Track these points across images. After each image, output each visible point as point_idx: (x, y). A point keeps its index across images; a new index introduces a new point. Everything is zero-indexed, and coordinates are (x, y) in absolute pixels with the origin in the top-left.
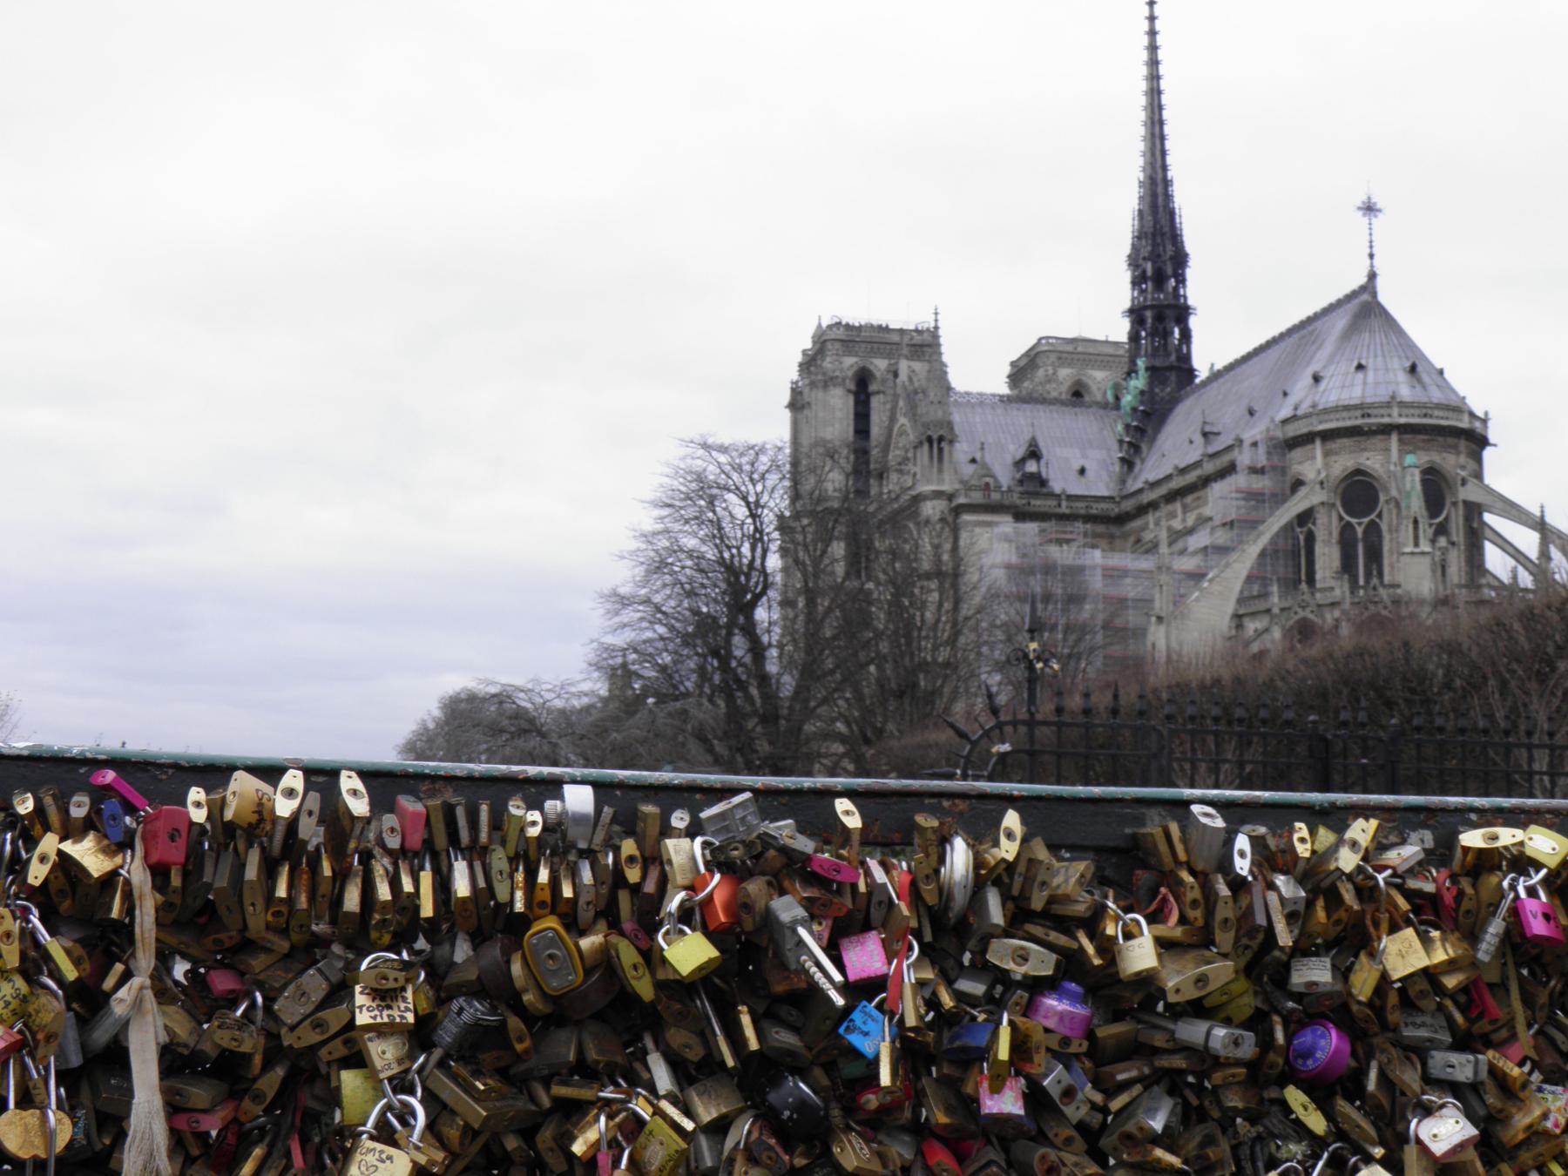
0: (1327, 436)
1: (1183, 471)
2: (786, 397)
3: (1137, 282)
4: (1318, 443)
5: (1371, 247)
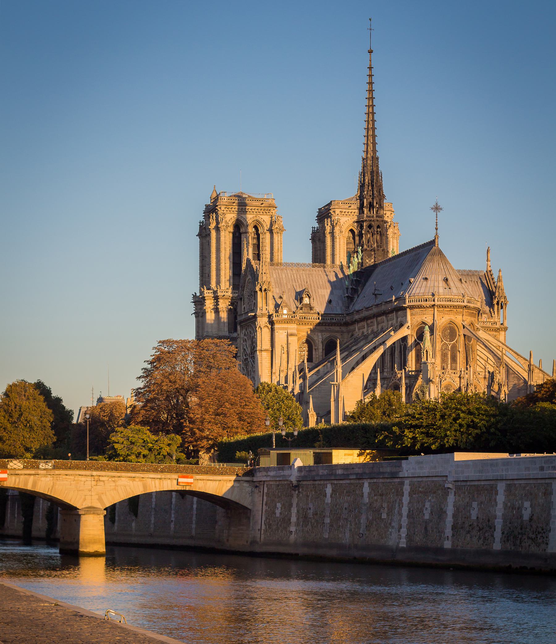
0: (412, 307)
1: (367, 309)
2: (197, 231)
5: (437, 225)
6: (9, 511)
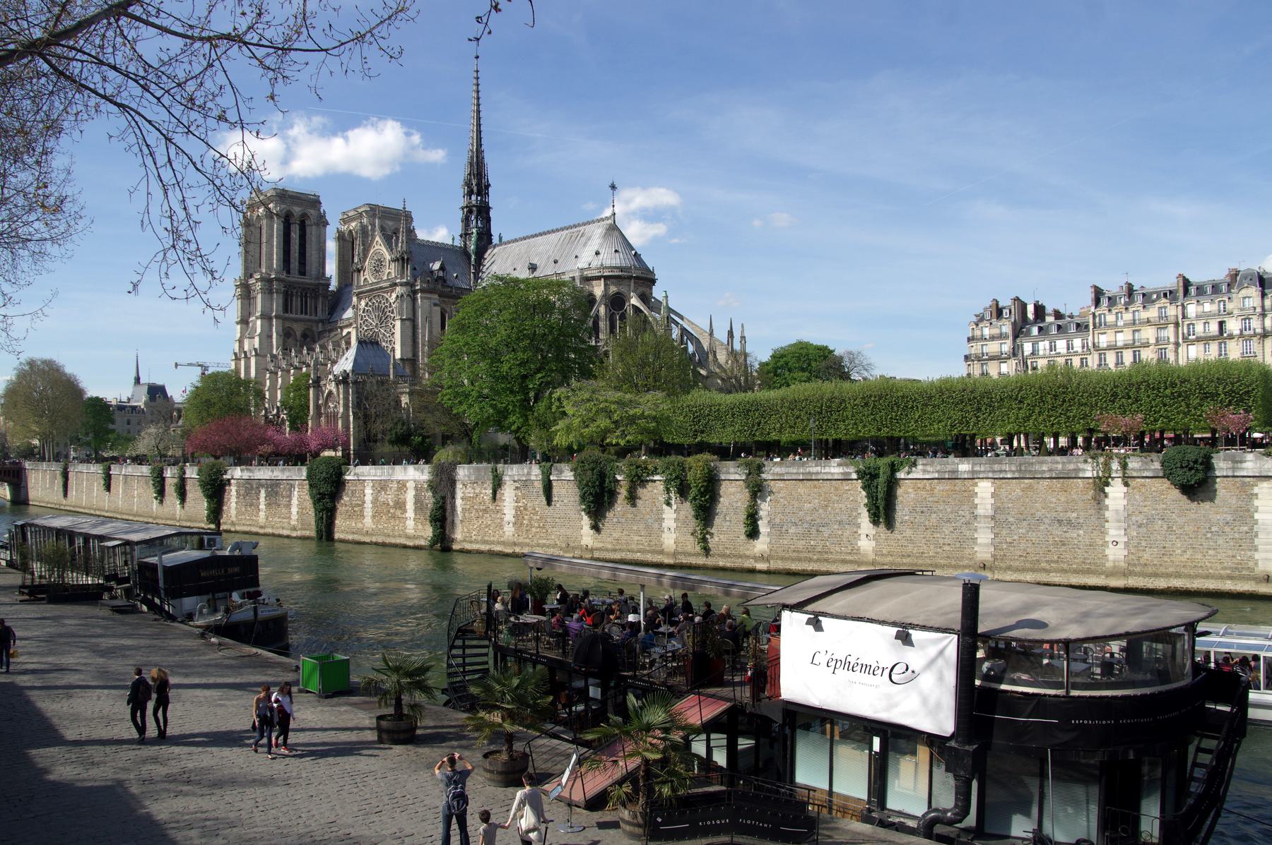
0: (606, 278)
3: (470, 193)
4: (603, 279)
6: (234, 499)
